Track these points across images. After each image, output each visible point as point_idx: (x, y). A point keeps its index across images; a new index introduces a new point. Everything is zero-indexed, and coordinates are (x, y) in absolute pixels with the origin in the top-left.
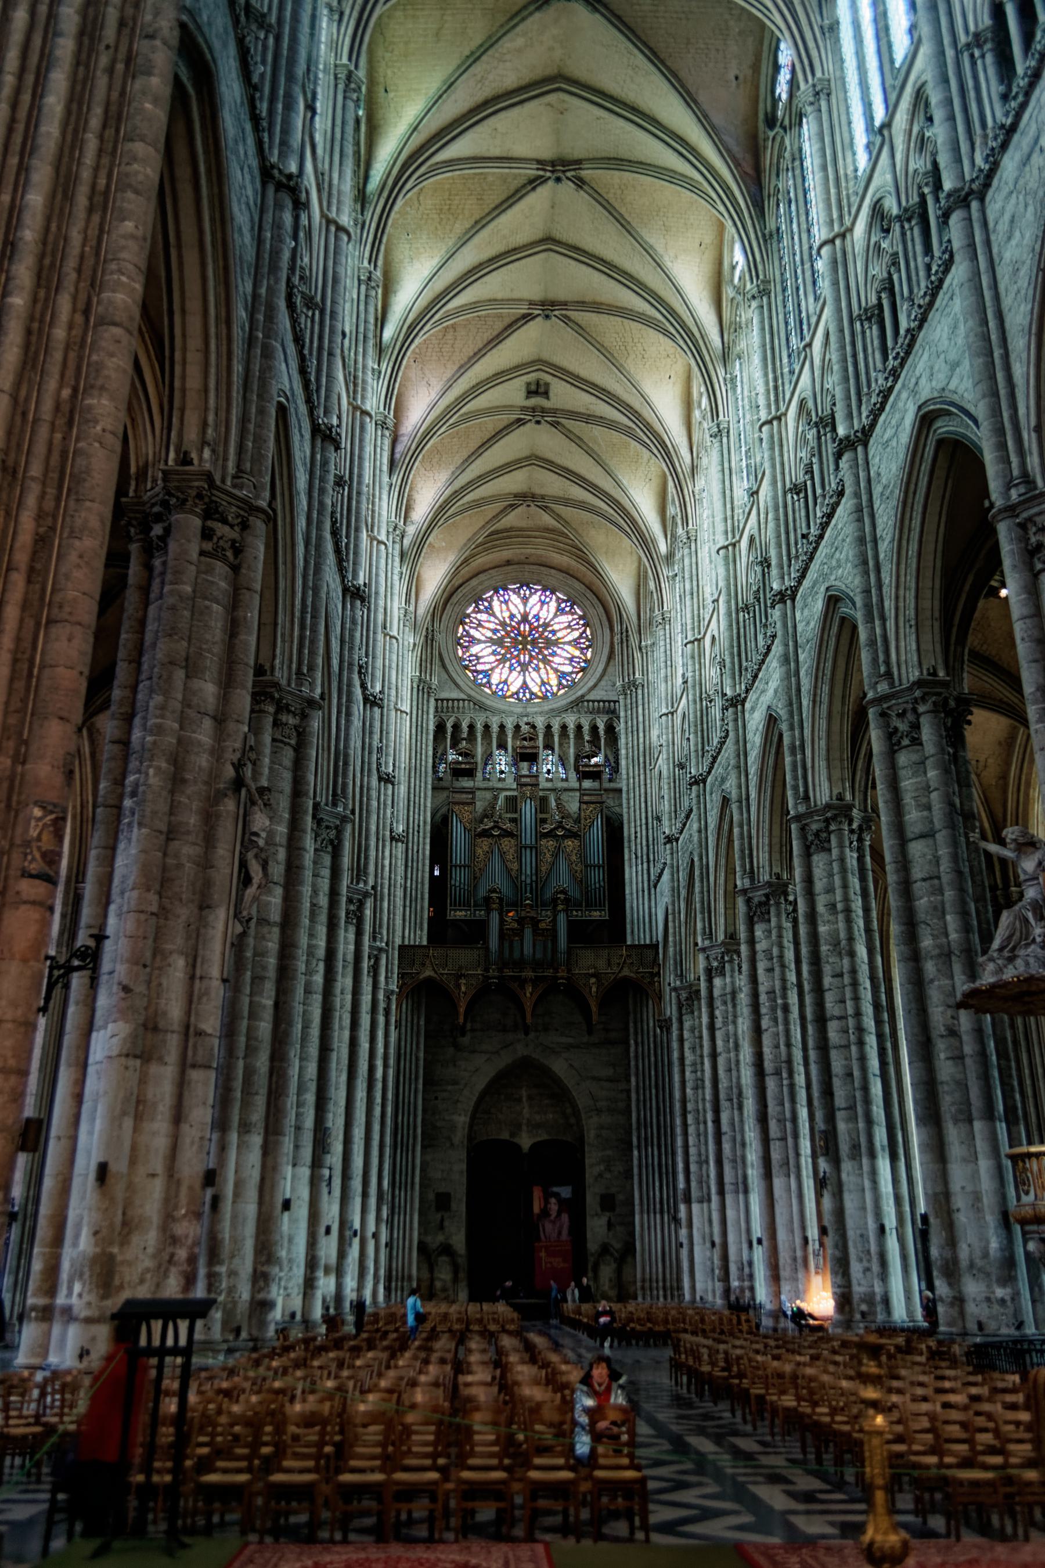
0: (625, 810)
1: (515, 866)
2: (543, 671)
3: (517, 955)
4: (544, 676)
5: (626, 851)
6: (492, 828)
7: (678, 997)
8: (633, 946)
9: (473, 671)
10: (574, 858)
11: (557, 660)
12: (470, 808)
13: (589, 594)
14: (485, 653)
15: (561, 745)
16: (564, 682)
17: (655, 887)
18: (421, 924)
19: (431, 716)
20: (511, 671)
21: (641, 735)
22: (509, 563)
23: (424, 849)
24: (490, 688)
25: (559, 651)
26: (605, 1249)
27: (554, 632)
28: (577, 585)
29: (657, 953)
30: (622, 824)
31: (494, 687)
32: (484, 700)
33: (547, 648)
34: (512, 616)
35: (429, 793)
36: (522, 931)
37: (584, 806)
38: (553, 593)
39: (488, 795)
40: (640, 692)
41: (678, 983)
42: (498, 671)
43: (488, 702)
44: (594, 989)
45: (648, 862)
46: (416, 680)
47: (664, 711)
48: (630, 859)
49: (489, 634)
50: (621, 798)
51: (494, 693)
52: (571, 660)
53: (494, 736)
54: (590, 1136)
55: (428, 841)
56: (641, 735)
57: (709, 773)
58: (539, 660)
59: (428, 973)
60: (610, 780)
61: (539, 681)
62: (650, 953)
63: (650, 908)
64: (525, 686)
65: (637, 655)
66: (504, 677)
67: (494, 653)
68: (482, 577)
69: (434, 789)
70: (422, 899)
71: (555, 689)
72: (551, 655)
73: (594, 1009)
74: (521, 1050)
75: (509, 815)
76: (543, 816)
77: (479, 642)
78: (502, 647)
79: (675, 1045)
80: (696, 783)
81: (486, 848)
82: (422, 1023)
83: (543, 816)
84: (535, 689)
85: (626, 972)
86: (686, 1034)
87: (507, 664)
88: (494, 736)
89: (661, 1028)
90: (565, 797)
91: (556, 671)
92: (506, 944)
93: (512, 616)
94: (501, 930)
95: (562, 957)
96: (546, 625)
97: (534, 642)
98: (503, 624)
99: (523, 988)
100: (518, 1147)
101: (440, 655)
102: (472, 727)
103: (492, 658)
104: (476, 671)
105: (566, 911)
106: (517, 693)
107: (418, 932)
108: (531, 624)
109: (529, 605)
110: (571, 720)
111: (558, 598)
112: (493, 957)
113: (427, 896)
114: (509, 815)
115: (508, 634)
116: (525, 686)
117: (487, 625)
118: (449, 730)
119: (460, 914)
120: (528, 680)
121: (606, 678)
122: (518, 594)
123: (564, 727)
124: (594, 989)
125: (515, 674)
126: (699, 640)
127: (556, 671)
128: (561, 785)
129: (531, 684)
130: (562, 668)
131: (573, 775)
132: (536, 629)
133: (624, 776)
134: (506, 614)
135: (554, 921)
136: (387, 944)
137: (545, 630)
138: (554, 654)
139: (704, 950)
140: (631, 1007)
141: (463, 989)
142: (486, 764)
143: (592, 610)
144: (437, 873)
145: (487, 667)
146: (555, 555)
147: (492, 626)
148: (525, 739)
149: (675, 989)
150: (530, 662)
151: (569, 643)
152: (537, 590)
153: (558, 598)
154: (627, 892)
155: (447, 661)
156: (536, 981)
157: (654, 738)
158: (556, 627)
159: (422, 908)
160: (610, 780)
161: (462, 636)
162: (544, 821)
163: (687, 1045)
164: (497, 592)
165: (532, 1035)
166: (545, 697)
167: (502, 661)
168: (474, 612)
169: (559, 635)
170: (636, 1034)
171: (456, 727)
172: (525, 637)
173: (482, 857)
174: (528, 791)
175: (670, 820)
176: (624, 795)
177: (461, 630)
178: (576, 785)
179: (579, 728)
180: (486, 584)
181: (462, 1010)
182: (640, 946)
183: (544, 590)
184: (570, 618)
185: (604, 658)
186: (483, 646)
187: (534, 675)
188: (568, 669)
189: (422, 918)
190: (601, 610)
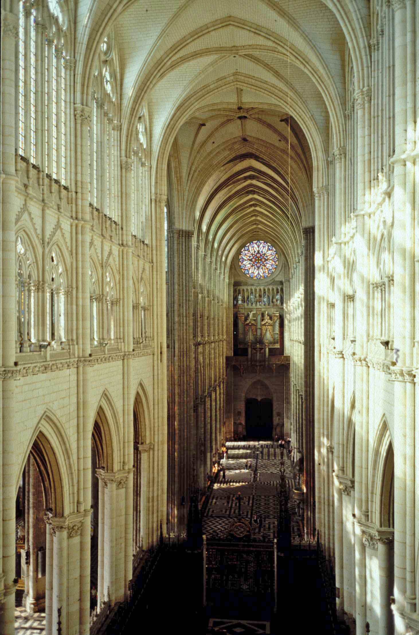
26: (278, 425)
27: (267, 256)
54: (275, 399)
64: (259, 274)
67: (250, 264)
74: (258, 378)
84: (262, 275)
91: (267, 269)
96: (265, 254)
97: (261, 260)
98: (252, 254)
100: (257, 400)
110: (270, 287)
115: (253, 258)
116: (259, 274)
119: (241, 346)
129: (260, 273)
138: (267, 263)
156: (260, 366)
158: (268, 255)
167: (252, 266)
187: (261, 270)
188: (271, 268)
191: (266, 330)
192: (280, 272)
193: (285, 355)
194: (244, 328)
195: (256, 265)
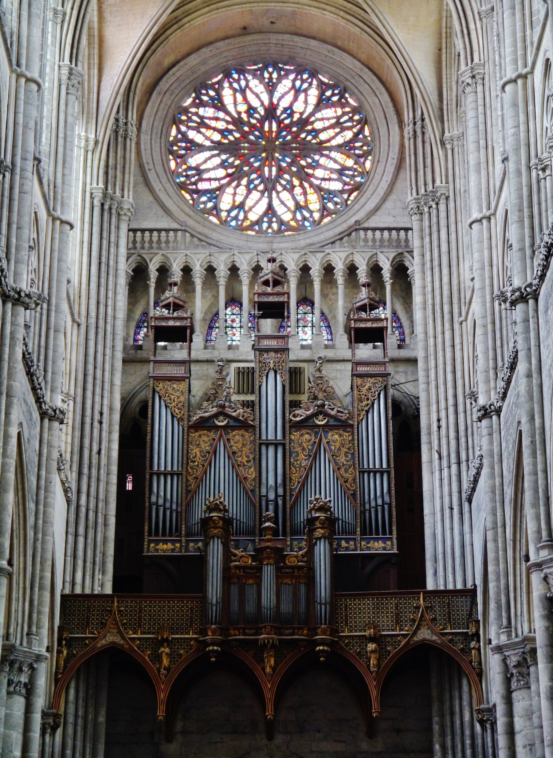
0: (422, 386)
1: (252, 473)
2: (298, 191)
3: (250, 607)
4: (301, 199)
5: (424, 448)
6: (216, 416)
7: (504, 661)
8: (436, 593)
9: (192, 192)
10: (342, 459)
11: (319, 173)
12: (183, 386)
13: (368, 75)
14: (209, 165)
15: (324, 295)
16: (330, 205)
17: (470, 501)
18: (104, 563)
19: (123, 251)
20: (249, 192)
21: (445, 271)
22: (245, 31)
23: (109, 449)
24: (218, 216)
25: (323, 161)
27: (316, 133)
28: (349, 61)
29: (474, 602)
30: (418, 410)
31: (224, 215)
32: (206, 231)
33: (304, 157)
34: (251, 110)
35: (119, 364)
36: (259, 569)
37: (359, 381)
38: (313, 75)
39: (211, 370)
40: (442, 207)
41: (504, 639)
42: (230, 190)
43: (215, 235)
44: (373, 662)
45: (459, 463)
46: (98, 195)
47: (476, 215)
48: (431, 461)
49: (217, 137)
50: (416, 371)
51: (224, 223)
52: (341, 172)
53: (222, 282)
55: (116, 436)
56: (445, 271)
57: (542, 277)
58: (292, 175)
59: (111, 638)
60: (400, 347)
61: (291, 204)
62: (463, 603)
63: (462, 534)
65: (438, 152)
66: (239, 199)
67: (223, 165)
68: (206, 52)
69: (124, 361)
70: (106, 525)
71: (317, 216)
72: (309, 166)
73: (374, 693)
75: (242, 398)
76: (295, 397)
77: (201, 148)
78: (238, 156)
79: (502, 741)
80: (523, 299)
81: (206, 447)
82: (102, 719)
83: (295, 397)
85: (425, 634)
86: (519, 723)
87: (244, 182)
88: (222, 282)
89: (482, 723)
90: (328, 371)
91: (318, 189)
92: (234, 590)
93: (251, 110)
94: (226, 569)
95: (322, 610)
96: (304, 122)
98: (238, 122)
99: (261, 661)
101: (141, 166)
102: (187, 270)
103: (221, 173)
104: (197, 191)
105: (329, 538)
106: (259, 222)
107: (98, 576)
108: (280, 123)
109: (277, 95)
111: (321, 83)
112: (214, 611)
113: (112, 521)
114: (242, 398)
115: (244, 135)
117: (213, 123)
118: (153, 275)
119: (165, 548)
120: (276, 203)
121: (393, 197)
122: (261, 79)
123: (329, 270)
124: (373, 662)
125: (255, 195)
126: (524, 77)
127: (318, 189)
128: (324, 353)
129: (280, 209)
130: (326, 185)
131: (342, 339)
132: (288, 128)
133: (420, 336)
134: (243, 108)
135: (310, 553)
136: (10, 563)
137: (301, 130)
138: (316, 165)
139: (539, 566)
140: (435, 693)
141: (165, 662)
142: (211, 328)
143: (372, 99)
144: (129, 486)
145: (215, 185)
146: (314, 11)
147: (221, 125)
148: (266, 283)
149: (499, 649)
150: (279, 175)
151: (339, 148)
152: (288, 73)
153: (321, 83)
154: (427, 510)
155: (152, 176)
157: (466, 275)
158: (318, 125)
159: (105, 539)
160: (400, 347)
161: (176, 141)
162: (295, 404)
163: (520, 741)
164: (228, 75)
165: (279, 739)
166: (300, 228)
168: (194, 104)
169: (323, 136)
170: (443, 734)
171: (163, 271)
172: (270, 141)
173: (199, 459)
174: (271, 359)
175: (488, 381)
176: (420, 364)
177: (174, 132)
178: (348, 354)
179: (352, 269)
180: (212, 63)
181: (162, 696)
182: (446, 592)
183: (299, 72)
184: (339, 111)
185: (391, 169)
186: (208, 154)
187: (285, 196)
188: (336, 186)
189: (104, 554)
190: (385, 97)
191: (315, 457)
192: (384, 200)
193: (430, 585)
194: (186, 443)
195: (259, 170)
